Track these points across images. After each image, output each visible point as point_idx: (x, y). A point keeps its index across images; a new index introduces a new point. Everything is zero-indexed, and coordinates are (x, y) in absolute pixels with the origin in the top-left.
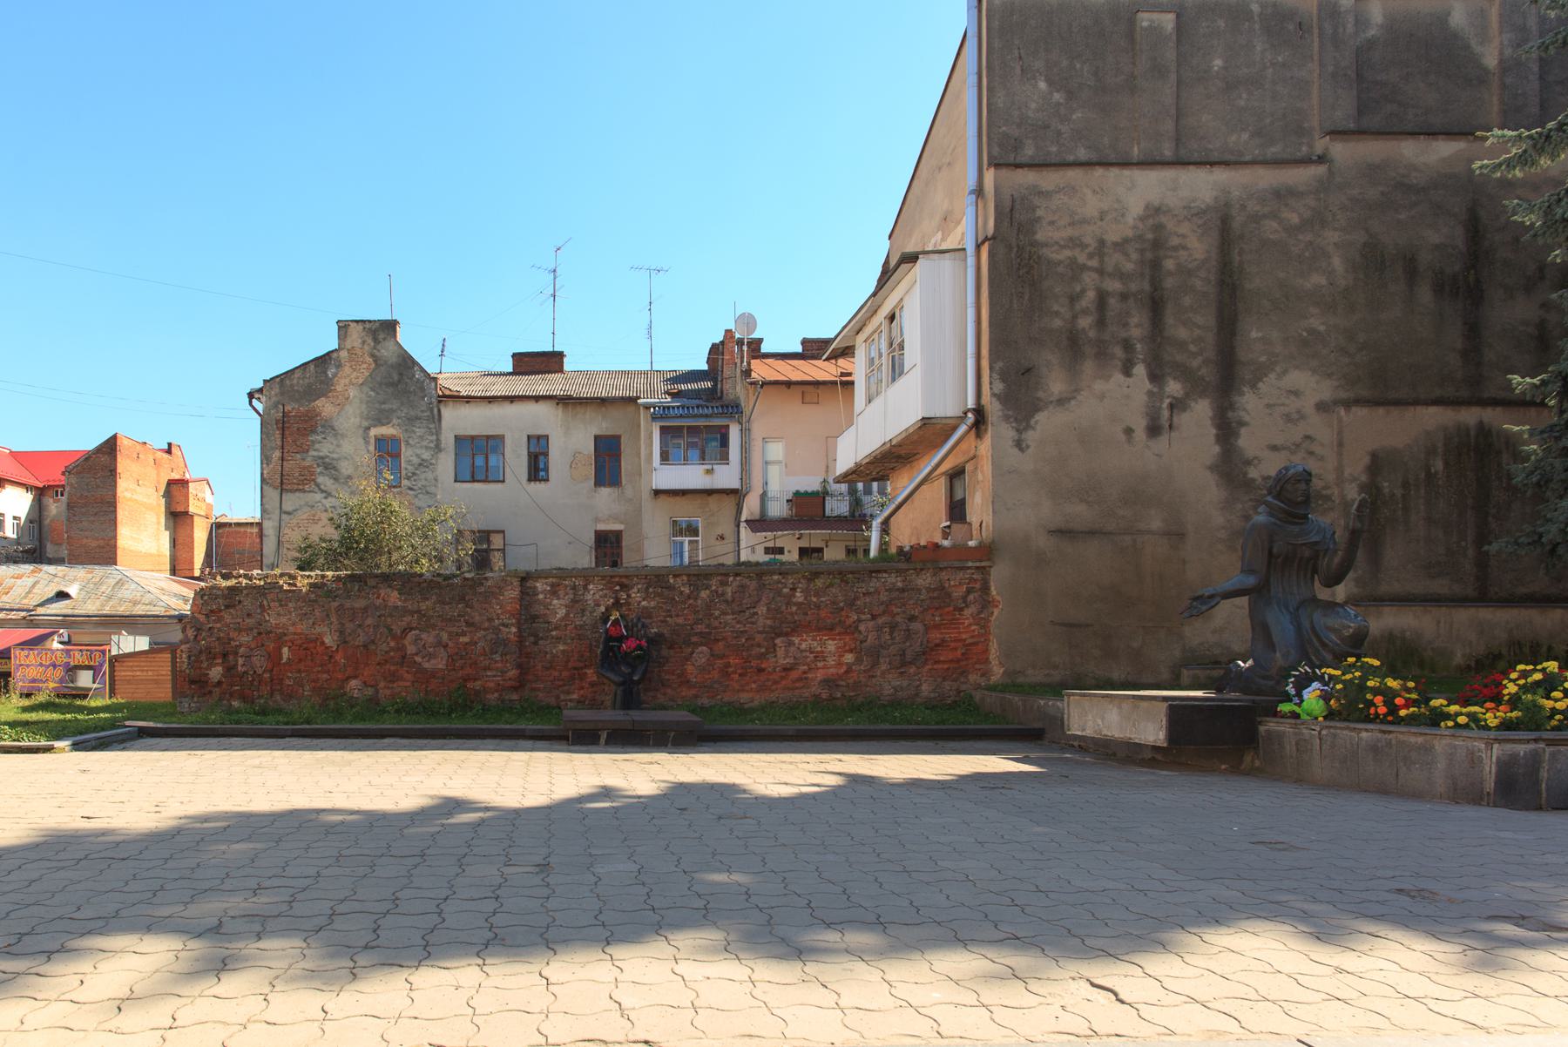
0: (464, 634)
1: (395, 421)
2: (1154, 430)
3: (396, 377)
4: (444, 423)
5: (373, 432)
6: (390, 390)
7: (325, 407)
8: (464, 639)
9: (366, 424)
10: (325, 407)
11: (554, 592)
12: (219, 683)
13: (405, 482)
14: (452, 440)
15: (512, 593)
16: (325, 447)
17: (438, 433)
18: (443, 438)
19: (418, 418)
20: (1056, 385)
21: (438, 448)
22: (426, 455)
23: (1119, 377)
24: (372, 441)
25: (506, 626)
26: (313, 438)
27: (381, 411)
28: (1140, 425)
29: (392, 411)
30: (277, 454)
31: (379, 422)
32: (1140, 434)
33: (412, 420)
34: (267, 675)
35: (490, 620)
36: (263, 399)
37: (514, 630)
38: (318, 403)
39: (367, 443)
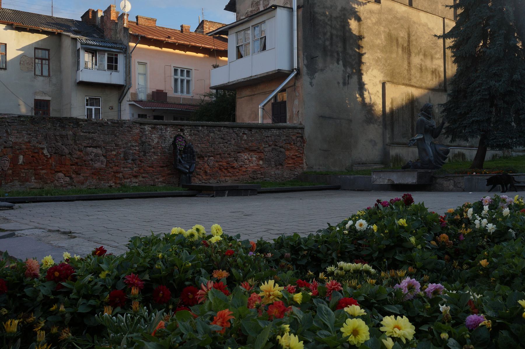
0: (114, 150)
2: (344, 84)
20: (320, 64)
23: (336, 64)
25: (133, 146)
28: (341, 81)
32: (341, 84)
35: (126, 143)
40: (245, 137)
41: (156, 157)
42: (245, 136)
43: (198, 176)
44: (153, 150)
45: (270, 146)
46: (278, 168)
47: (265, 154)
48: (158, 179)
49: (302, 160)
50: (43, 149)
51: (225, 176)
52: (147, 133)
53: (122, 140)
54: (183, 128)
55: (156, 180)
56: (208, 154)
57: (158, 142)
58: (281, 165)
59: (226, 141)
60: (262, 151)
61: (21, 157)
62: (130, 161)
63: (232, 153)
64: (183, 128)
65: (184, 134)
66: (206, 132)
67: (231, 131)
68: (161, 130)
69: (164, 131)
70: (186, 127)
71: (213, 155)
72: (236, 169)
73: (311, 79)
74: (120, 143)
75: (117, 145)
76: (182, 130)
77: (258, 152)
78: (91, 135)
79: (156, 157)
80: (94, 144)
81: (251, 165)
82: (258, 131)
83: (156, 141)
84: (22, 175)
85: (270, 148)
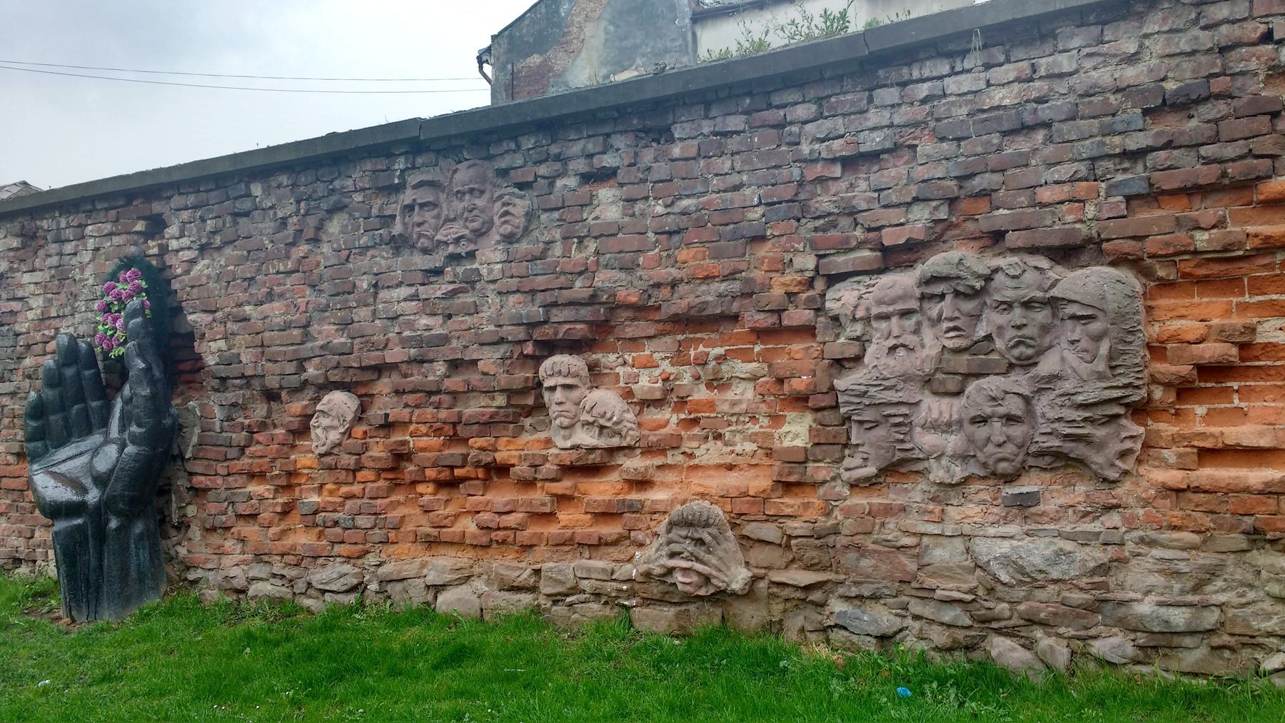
1: (639, 61)
29: (636, 47)
40: (608, 205)
42: (606, 194)
43: (249, 530)
44: (28, 362)
45: (895, 257)
46: (1024, 504)
47: (841, 345)
51: (432, 543)
54: (157, 207)
56: (311, 371)
57: (44, 318)
58: (1063, 461)
59: (437, 260)
60: (798, 316)
63: (489, 359)
64: (157, 207)
65: (164, 250)
68: (60, 241)
69: (69, 248)
70: (177, 201)
71: (335, 376)
72: (528, 484)
76: (157, 226)
77: (761, 334)
81: (710, 453)
82: (736, 122)
83: (37, 303)
85: (903, 281)
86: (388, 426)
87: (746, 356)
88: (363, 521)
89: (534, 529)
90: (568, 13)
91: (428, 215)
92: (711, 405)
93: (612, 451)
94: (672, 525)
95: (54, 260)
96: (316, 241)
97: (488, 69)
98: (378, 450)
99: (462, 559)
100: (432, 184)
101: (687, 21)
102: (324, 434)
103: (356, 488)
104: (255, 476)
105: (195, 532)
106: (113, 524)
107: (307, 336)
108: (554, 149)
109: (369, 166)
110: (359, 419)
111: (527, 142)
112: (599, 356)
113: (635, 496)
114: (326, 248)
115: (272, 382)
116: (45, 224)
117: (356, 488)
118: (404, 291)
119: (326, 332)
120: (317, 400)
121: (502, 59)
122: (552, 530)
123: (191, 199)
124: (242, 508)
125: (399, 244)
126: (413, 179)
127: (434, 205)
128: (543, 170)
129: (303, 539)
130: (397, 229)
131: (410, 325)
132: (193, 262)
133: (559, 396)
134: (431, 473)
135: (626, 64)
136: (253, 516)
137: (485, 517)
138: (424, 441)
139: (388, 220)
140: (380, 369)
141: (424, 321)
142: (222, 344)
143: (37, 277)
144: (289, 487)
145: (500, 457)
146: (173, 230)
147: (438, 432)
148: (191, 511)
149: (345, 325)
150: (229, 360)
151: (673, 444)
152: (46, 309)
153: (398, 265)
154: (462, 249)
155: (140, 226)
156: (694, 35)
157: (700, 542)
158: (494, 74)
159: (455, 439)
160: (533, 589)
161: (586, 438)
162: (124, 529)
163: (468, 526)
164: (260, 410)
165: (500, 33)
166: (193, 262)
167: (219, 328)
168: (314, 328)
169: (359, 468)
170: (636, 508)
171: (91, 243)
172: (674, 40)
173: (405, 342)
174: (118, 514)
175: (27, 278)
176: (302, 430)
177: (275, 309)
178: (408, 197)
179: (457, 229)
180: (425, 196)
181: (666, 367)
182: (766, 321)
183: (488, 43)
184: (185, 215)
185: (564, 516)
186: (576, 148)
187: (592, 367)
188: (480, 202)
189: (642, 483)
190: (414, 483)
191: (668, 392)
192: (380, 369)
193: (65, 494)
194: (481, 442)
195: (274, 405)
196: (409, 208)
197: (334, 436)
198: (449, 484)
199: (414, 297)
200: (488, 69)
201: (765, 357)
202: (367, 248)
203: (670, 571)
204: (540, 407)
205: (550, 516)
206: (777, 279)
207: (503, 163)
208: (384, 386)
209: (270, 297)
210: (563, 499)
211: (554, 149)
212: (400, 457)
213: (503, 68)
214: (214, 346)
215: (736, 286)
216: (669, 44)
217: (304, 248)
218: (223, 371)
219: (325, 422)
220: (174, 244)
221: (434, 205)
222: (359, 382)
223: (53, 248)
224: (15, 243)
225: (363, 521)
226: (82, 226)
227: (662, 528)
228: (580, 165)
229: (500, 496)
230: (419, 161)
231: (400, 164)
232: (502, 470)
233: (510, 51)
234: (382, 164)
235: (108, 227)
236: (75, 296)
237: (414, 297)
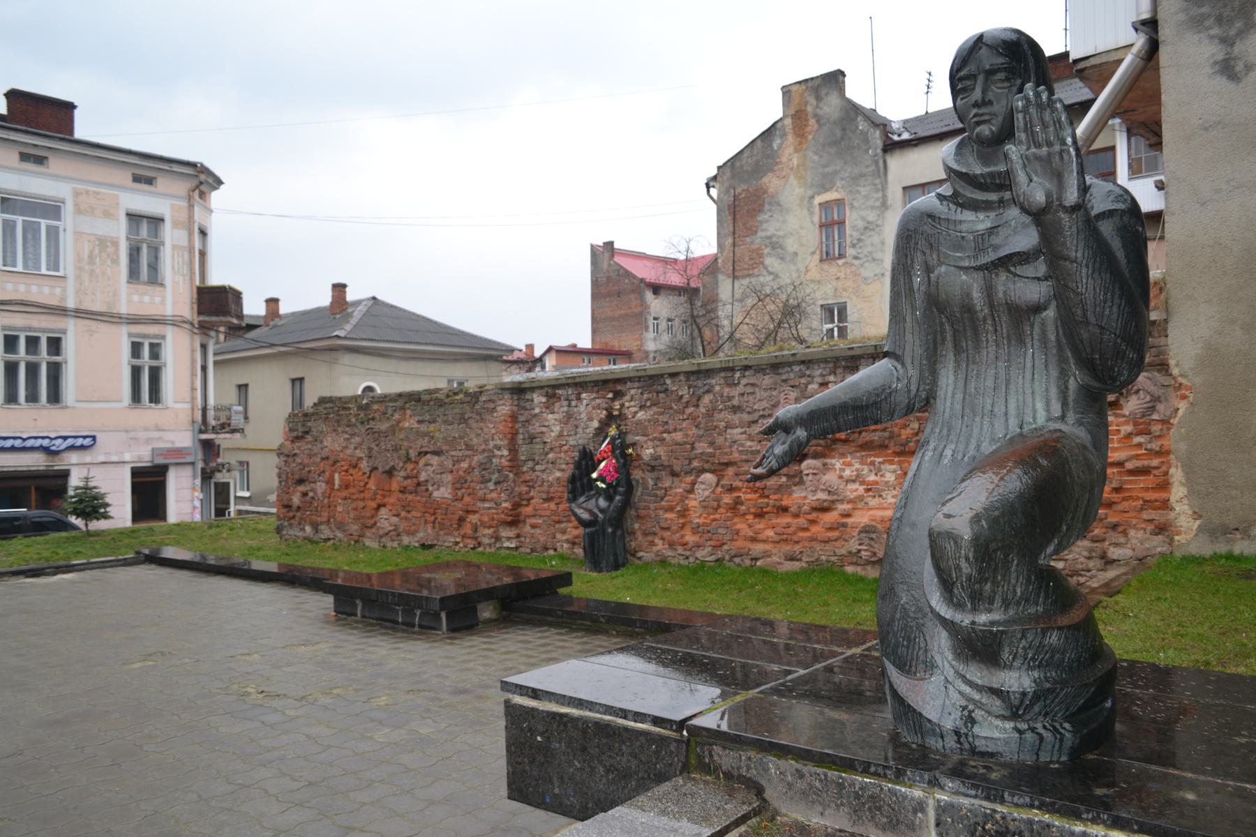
1: (839, 184)
3: (839, 133)
4: (891, 176)
5: (818, 200)
6: (833, 150)
7: (771, 182)
8: (465, 465)
9: (810, 193)
10: (771, 182)
11: (548, 406)
12: (299, 508)
13: (850, 252)
14: (900, 192)
15: (504, 408)
16: (771, 225)
17: (884, 188)
18: (889, 193)
19: (862, 175)
21: (884, 206)
22: (872, 216)
24: (817, 210)
26: (761, 217)
27: (824, 176)
29: (836, 173)
30: (730, 240)
31: (824, 189)
33: (856, 179)
34: (326, 501)
35: (486, 442)
36: (717, 185)
37: (505, 453)
38: (765, 180)
39: (811, 213)
41: (558, 474)
43: (667, 534)
44: (551, 456)
48: (564, 532)
49: (1164, 486)
50: (360, 459)
52: (537, 410)
53: (478, 435)
55: (559, 536)
56: (695, 464)
57: (560, 435)
61: (337, 476)
62: (491, 486)
64: (619, 388)
65: (622, 405)
66: (684, 392)
67: (767, 380)
70: (629, 384)
72: (796, 516)
73: (1227, 41)
74: (475, 441)
75: (468, 447)
78: (424, 428)
79: (558, 474)
80: (432, 448)
83: (557, 429)
84: (340, 509)
86: (731, 489)
87: (891, 462)
88: (720, 531)
89: (801, 534)
90: (780, 146)
91: (751, 398)
92: (876, 483)
93: (833, 502)
94: (860, 532)
95: (565, 409)
96: (697, 406)
97: (714, 192)
98: (727, 499)
99: (767, 547)
100: (753, 385)
101: (879, 151)
102: (702, 492)
103: (717, 516)
104: (670, 509)
105: (639, 534)
106: (610, 530)
107: (693, 449)
108: (808, 372)
109: (723, 374)
110: (717, 485)
111: (796, 368)
112: (828, 461)
113: (844, 520)
114: (703, 410)
115: (677, 468)
116: (560, 392)
117: (717, 516)
118: (739, 430)
119: (702, 447)
120: (698, 476)
121: (726, 184)
122: (808, 534)
123: (636, 384)
124: (663, 525)
125: (736, 409)
126: (744, 381)
127: (753, 393)
128: (803, 381)
129: (690, 538)
130: (735, 402)
131: (742, 445)
132: (636, 413)
133: (810, 477)
134: (752, 510)
135: (828, 186)
136: (668, 529)
137: (779, 530)
138: (749, 496)
139: (730, 398)
140: (727, 464)
141: (749, 443)
142: (651, 451)
143: (556, 416)
144: (683, 516)
145: (784, 503)
146: (628, 397)
147: (755, 492)
148: (636, 526)
149: (712, 444)
150: (656, 458)
151: (861, 498)
152: (561, 432)
153: (736, 418)
154: (766, 413)
155: (610, 395)
156: (885, 162)
157: (872, 539)
158: (719, 195)
159: (762, 496)
160: (800, 560)
161: (822, 496)
162: (614, 533)
163: (770, 533)
164: (667, 483)
165: (725, 164)
166: (636, 413)
167: (650, 443)
168: (697, 445)
169: (719, 506)
170: (844, 525)
171: (585, 402)
172: (867, 167)
173: (741, 452)
174: (611, 525)
175: (550, 416)
176: (691, 491)
177: (678, 436)
178: (740, 389)
179: (765, 404)
180: (749, 389)
181: (857, 466)
182: (898, 449)
183: (715, 172)
184: (633, 392)
185: (814, 529)
186: (818, 372)
187: (824, 465)
188: (774, 393)
189: (848, 516)
190: (745, 514)
191: (857, 476)
192: (727, 464)
193: (585, 516)
194: (776, 497)
195: (676, 479)
196: (743, 394)
197: (707, 493)
198: (760, 515)
199: (744, 433)
200: (714, 192)
201: (900, 463)
202: (721, 410)
203: (859, 551)
204: (801, 482)
205: (806, 529)
206: (903, 431)
207: (784, 377)
208: (731, 471)
209: (675, 430)
210: (813, 522)
211: (808, 372)
212: (738, 502)
213: (727, 192)
214: (648, 452)
215: (887, 434)
216: (864, 170)
217: (690, 410)
218: (653, 463)
219: (703, 487)
220: (627, 404)
221: (753, 393)
222: (719, 469)
223: (565, 403)
224: (544, 400)
225: (720, 531)
226: (579, 394)
227: (855, 534)
228: (820, 380)
229: (785, 520)
230: (747, 373)
231: (738, 375)
232: (785, 510)
233: (733, 177)
234: (729, 374)
235: (594, 395)
236: (577, 427)
237: (744, 433)
